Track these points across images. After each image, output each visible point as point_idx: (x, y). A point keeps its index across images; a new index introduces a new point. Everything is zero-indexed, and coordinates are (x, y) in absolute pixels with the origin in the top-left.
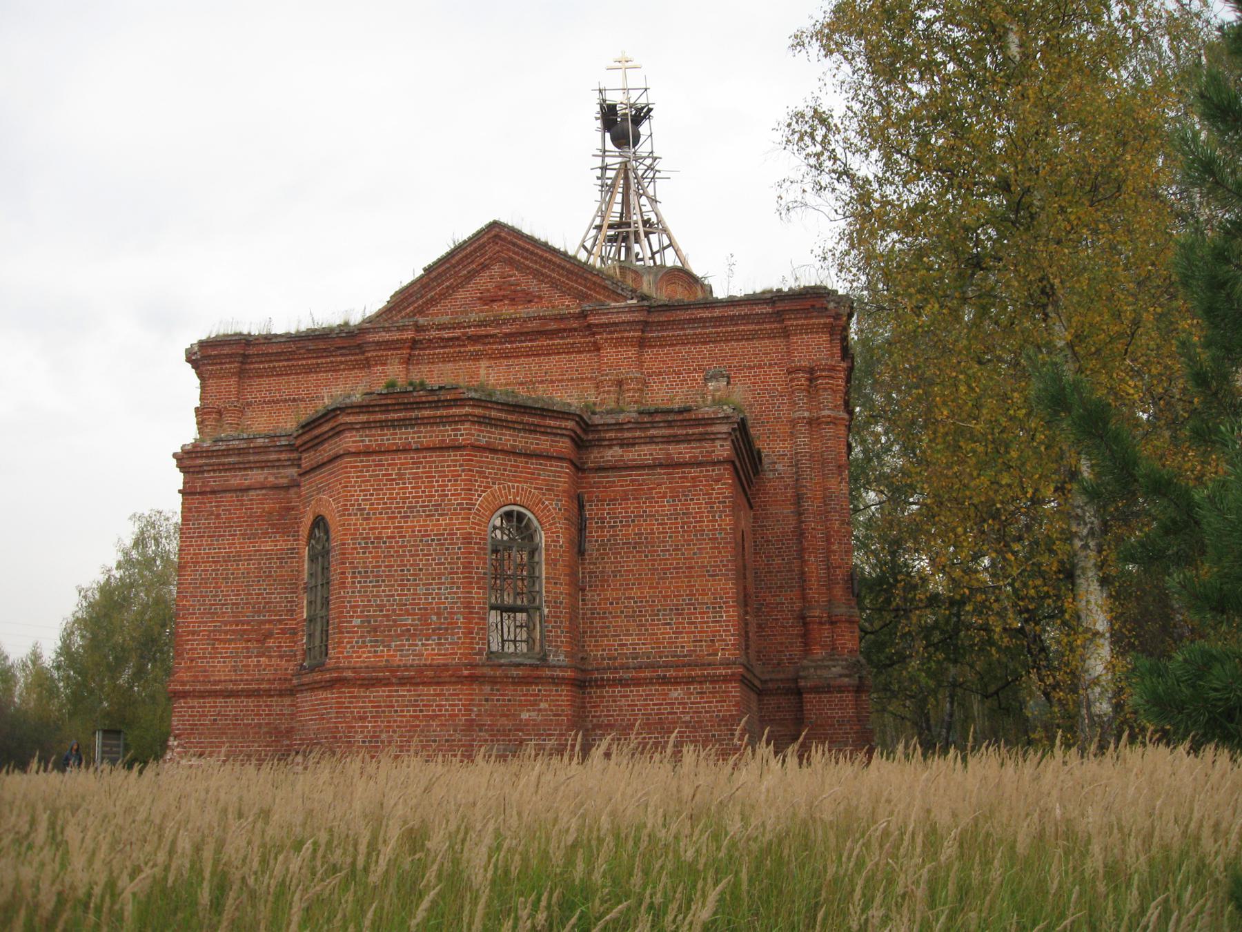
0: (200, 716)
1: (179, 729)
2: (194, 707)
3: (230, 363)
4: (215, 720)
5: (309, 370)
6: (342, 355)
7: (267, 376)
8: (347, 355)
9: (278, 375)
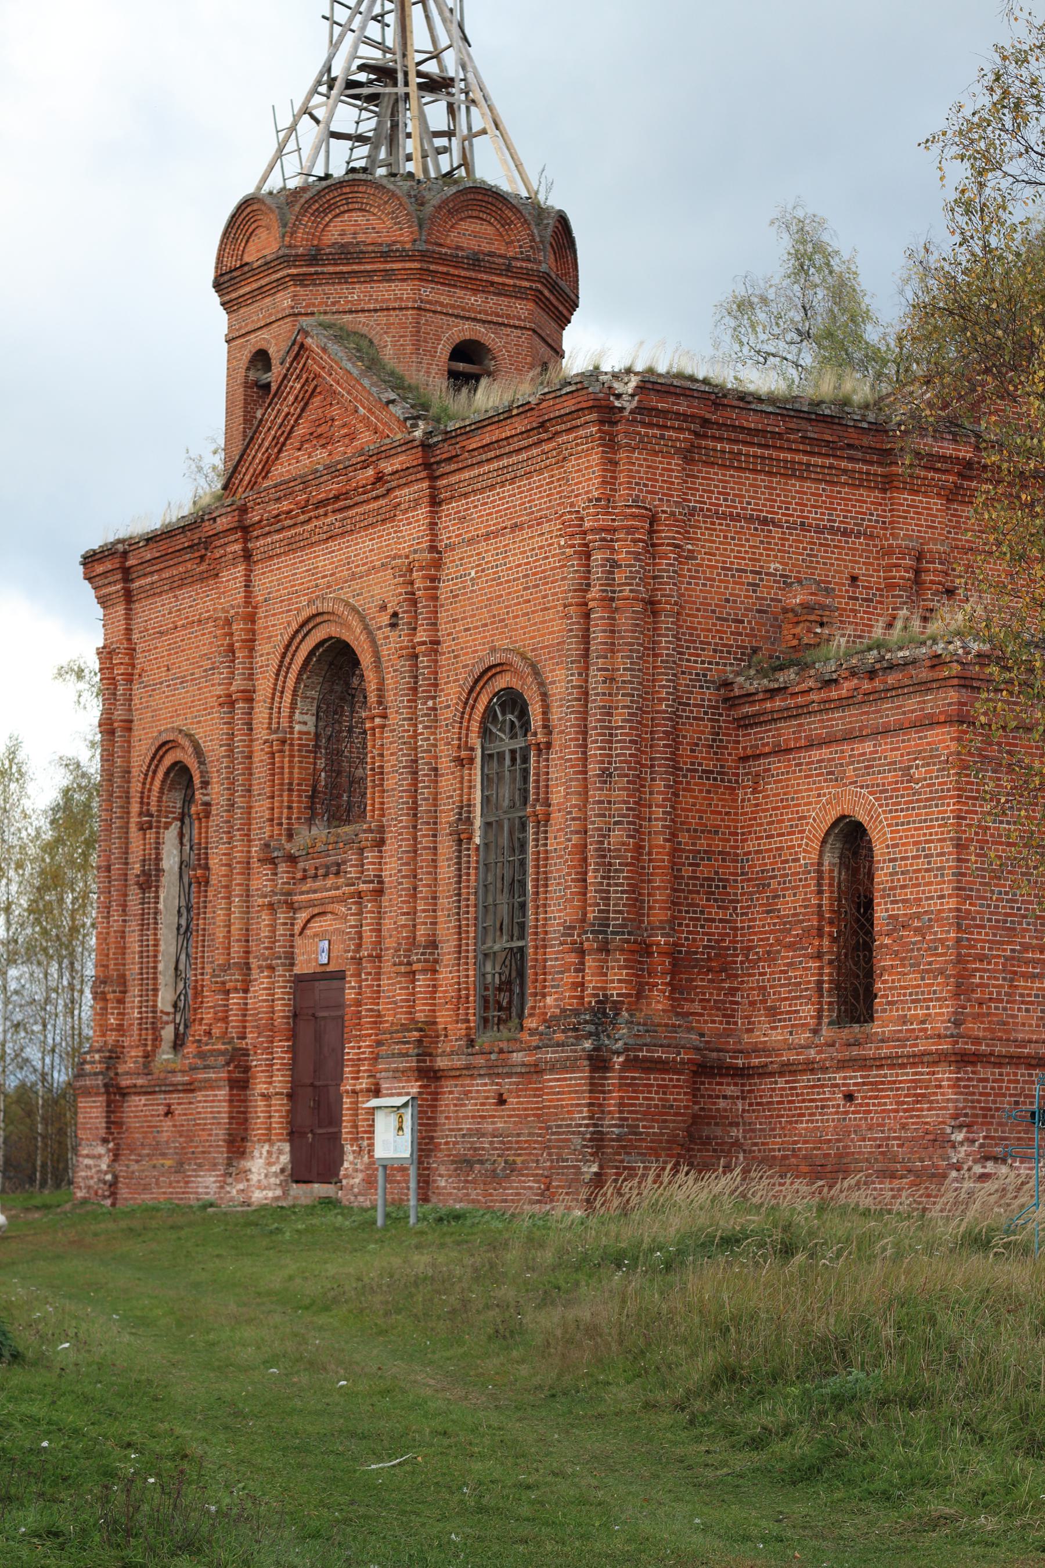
0: (996, 1095)
1: (966, 1115)
2: (986, 1080)
3: (680, 429)
4: (1017, 1103)
5: (792, 471)
6: (851, 459)
7: (723, 466)
8: (857, 460)
9: (739, 469)
